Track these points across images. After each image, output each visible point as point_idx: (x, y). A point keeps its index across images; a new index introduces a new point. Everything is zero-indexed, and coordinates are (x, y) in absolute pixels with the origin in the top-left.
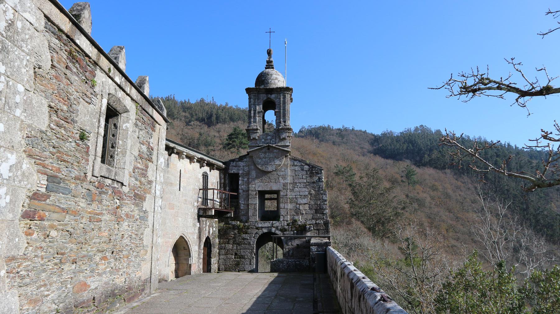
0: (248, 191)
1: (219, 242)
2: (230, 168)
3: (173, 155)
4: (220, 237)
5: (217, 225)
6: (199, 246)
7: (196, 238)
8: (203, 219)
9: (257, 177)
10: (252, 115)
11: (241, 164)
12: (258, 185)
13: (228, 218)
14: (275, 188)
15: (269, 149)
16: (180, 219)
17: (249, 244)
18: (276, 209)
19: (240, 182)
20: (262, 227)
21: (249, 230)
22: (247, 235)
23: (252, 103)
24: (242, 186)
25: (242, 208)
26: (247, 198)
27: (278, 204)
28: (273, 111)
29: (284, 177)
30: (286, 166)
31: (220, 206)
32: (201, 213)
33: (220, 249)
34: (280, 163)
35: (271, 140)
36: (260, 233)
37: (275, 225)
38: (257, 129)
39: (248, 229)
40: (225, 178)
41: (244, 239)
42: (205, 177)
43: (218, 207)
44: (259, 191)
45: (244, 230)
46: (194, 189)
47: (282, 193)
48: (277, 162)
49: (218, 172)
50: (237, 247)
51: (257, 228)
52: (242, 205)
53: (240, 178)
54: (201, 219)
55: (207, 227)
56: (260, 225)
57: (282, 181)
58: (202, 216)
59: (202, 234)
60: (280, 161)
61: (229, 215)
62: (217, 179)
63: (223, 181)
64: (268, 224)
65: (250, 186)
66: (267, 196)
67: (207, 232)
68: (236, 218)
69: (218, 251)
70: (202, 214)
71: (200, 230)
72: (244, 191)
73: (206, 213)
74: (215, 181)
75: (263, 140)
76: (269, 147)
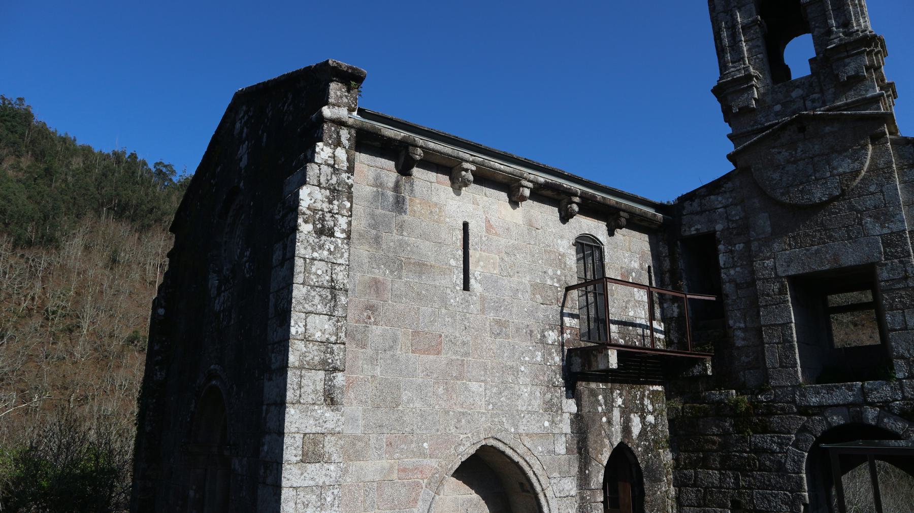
0: (752, 283)
1: (676, 459)
2: (685, 220)
3: (416, 171)
4: (674, 443)
5: (661, 405)
6: (583, 480)
7: (561, 448)
8: (593, 385)
9: (778, 232)
10: (726, 42)
11: (718, 201)
12: (784, 259)
13: (695, 379)
14: (851, 256)
15: (802, 129)
16: (474, 386)
17: (780, 469)
18: (879, 343)
19: (722, 259)
20: (821, 409)
21: (775, 419)
22: (768, 437)
23: (719, 8)
24: (730, 272)
25: (739, 343)
26: (753, 307)
27: (880, 322)
28: (810, 35)
29: (884, 214)
30: (881, 172)
31: (669, 343)
32: (576, 368)
33: (679, 483)
34: (856, 165)
35: (804, 98)
36: (819, 429)
37: (874, 397)
38: (749, 77)
39: (770, 413)
40: (672, 254)
41: (758, 450)
42: (587, 248)
43: (660, 346)
44: (789, 278)
45: (758, 419)
46: (537, 288)
47: (884, 274)
48: (845, 166)
49: (646, 237)
50: (736, 479)
51: (805, 410)
52: (739, 333)
53: (721, 247)
54: (581, 386)
55: (616, 413)
56: (814, 400)
57: (876, 230)
58: (588, 378)
59: (591, 438)
60: (858, 157)
61: (697, 370)
62: (642, 257)
63: (667, 264)
64: (843, 394)
65: (757, 265)
66: (836, 299)
67: (617, 428)
68: (722, 379)
69: (672, 491)
70: (579, 370)
71: (582, 428)
72: (738, 286)
73: (590, 366)
74: (636, 265)
75: (778, 108)
76: (801, 124)
